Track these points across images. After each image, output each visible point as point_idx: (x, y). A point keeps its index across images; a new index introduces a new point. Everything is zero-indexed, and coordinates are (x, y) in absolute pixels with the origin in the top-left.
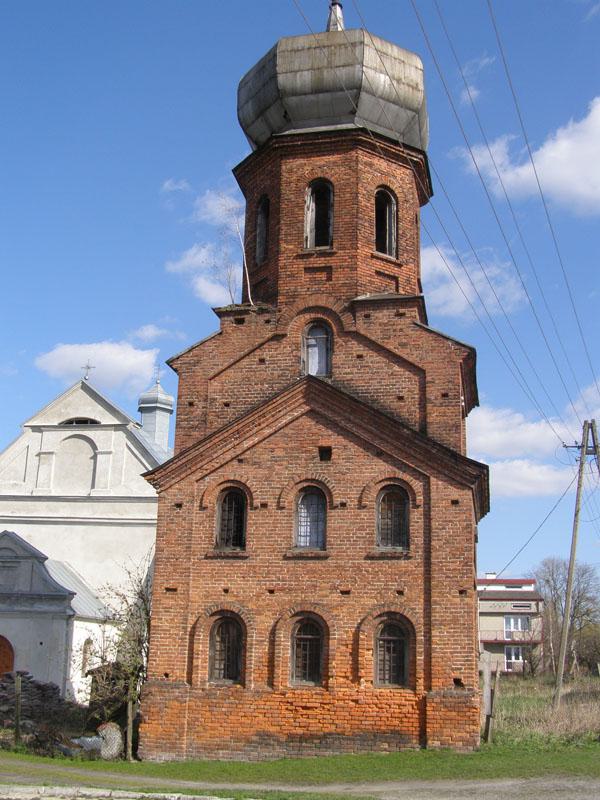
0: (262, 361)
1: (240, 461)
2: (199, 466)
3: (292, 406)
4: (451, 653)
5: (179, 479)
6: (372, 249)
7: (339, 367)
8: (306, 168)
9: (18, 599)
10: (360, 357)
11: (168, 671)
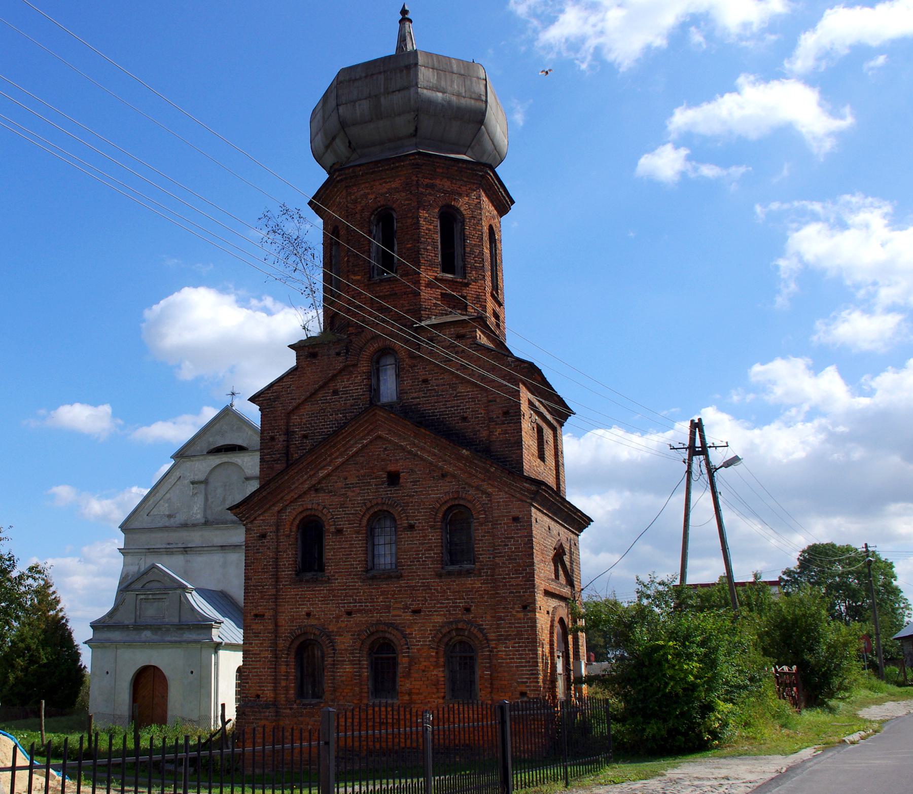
0: (335, 392)
1: (316, 490)
2: (279, 497)
3: (361, 435)
4: (517, 667)
5: (262, 510)
6: (436, 272)
7: (407, 393)
8: (370, 197)
9: (168, 630)
10: (425, 381)
11: (260, 692)
